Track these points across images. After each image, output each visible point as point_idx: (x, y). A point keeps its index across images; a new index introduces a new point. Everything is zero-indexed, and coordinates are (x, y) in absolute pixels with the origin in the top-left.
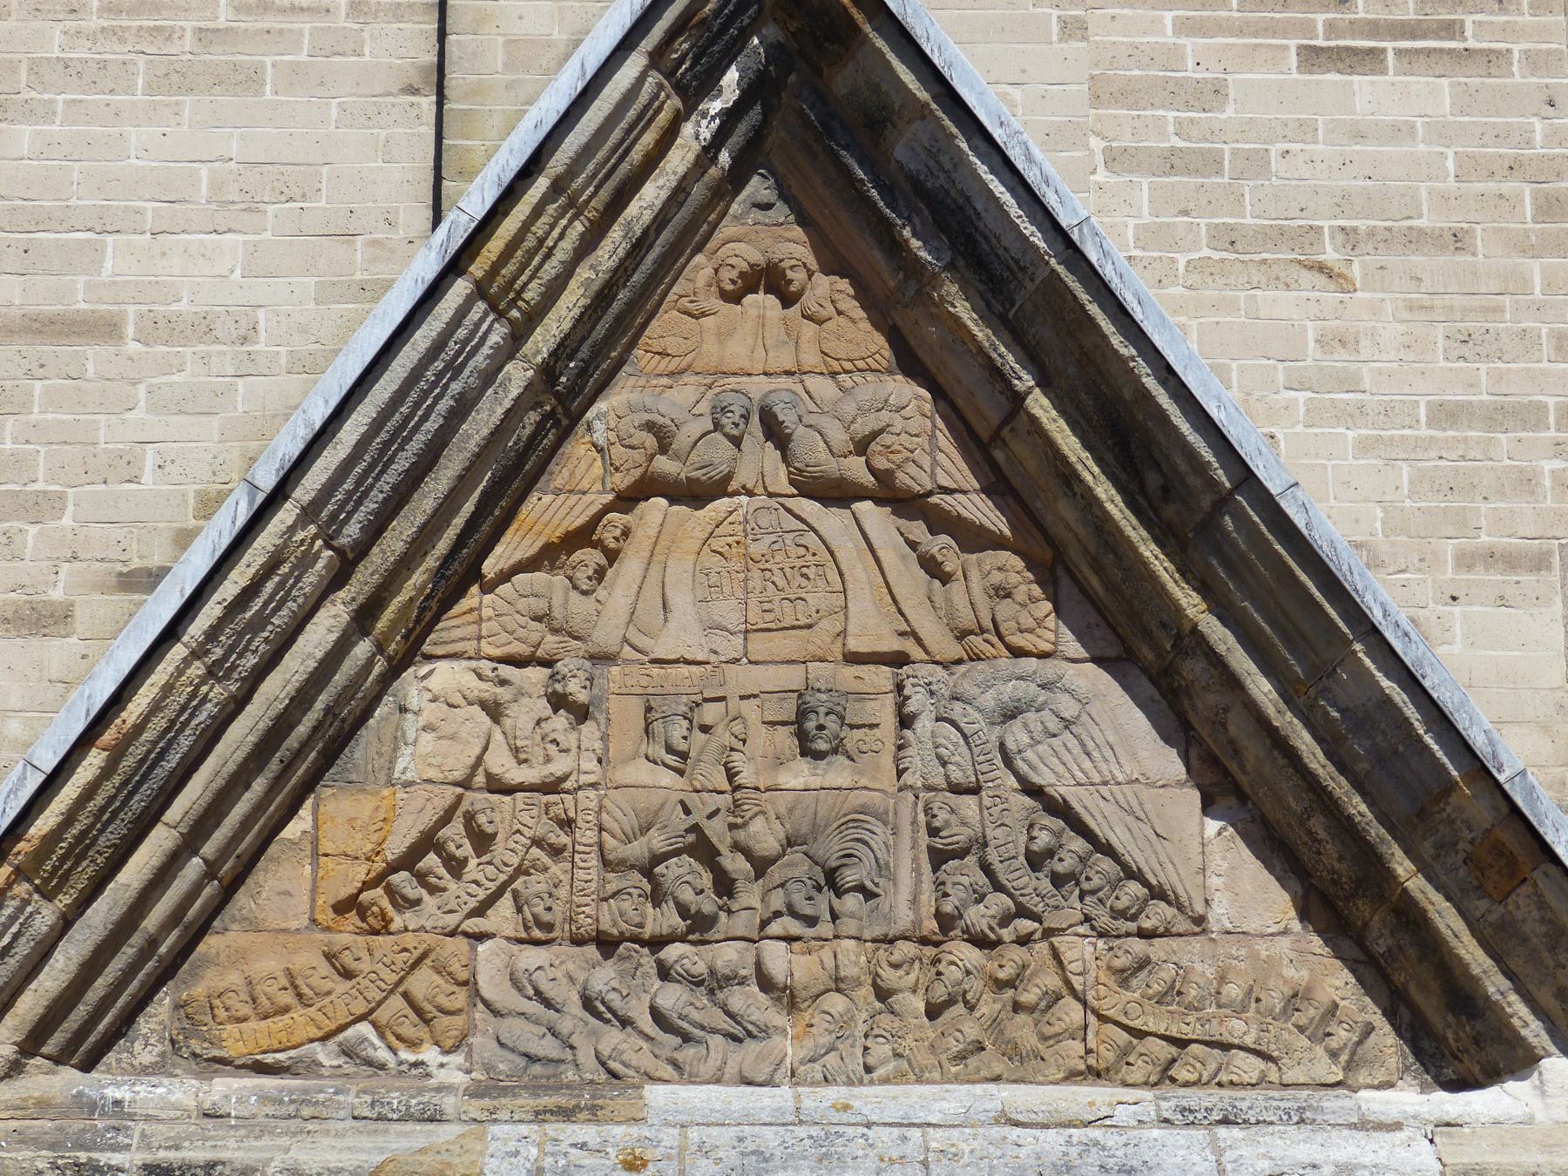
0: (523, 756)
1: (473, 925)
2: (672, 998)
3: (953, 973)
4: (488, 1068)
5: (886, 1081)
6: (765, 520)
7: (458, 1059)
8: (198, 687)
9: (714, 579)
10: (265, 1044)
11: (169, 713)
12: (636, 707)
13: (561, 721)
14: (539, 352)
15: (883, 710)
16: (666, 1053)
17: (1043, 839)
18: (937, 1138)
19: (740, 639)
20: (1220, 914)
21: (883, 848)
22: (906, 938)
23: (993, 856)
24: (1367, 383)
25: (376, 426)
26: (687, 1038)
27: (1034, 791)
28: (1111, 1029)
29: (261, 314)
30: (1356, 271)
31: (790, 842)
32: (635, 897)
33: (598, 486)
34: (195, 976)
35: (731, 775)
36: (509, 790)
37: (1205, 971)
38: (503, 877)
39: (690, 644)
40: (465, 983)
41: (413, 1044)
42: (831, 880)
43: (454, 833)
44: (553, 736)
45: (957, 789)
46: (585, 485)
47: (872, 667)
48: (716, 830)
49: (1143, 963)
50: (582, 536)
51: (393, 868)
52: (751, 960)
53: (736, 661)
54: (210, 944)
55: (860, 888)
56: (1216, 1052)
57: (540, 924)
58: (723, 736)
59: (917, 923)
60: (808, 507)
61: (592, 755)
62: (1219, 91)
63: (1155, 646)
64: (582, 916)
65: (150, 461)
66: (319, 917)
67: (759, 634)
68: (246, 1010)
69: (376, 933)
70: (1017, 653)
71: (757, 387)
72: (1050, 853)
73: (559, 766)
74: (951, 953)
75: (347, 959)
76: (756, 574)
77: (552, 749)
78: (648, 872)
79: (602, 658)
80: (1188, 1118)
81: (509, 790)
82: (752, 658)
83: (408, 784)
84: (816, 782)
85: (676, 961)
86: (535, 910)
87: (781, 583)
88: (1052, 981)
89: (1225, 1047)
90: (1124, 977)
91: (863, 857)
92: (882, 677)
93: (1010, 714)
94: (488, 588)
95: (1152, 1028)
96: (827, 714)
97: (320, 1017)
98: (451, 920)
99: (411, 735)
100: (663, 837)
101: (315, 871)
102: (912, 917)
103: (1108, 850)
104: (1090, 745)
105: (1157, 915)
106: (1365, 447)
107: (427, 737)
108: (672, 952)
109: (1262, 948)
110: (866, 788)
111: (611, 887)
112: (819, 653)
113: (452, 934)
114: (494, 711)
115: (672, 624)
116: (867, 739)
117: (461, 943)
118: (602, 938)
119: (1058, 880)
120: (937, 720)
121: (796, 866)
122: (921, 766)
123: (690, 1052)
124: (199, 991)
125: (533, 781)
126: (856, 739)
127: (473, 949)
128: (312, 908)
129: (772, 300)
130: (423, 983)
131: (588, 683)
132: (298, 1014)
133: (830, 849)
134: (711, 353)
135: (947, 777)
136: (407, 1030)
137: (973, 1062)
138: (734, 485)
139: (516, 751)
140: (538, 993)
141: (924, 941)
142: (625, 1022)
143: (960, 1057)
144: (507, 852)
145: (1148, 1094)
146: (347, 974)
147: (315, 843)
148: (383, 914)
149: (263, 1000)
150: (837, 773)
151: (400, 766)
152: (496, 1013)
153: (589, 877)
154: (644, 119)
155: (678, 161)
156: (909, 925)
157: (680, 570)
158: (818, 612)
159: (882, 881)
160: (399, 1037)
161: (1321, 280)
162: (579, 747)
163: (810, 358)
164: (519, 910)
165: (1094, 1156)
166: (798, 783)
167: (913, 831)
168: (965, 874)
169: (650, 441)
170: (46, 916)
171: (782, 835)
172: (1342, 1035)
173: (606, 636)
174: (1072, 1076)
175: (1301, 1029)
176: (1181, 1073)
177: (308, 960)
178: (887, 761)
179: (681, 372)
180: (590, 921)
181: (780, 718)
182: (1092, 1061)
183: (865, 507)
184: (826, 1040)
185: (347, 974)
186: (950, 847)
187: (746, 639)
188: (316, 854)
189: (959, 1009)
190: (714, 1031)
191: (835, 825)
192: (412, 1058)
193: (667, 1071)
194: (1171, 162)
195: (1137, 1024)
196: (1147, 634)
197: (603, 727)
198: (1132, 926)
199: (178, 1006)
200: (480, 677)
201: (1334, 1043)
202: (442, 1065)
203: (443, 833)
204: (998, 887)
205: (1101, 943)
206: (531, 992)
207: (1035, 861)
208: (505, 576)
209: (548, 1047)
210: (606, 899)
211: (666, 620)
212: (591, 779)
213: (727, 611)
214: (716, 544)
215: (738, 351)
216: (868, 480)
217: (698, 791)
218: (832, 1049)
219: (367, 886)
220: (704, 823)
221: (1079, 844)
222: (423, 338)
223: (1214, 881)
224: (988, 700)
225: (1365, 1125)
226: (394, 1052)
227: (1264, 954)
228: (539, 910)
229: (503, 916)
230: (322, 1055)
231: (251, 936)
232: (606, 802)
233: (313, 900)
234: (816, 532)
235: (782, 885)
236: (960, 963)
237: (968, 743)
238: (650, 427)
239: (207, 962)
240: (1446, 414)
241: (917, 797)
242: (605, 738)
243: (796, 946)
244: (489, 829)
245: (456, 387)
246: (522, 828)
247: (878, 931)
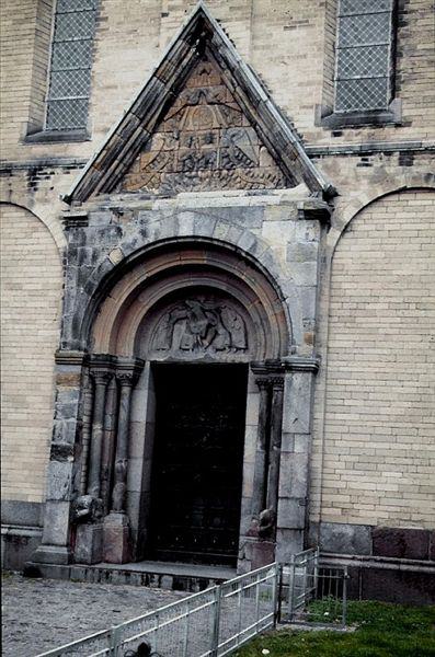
50: (178, 113)
62: (271, 35)
93: (234, 136)
114: (164, 140)
144: (166, 160)
150: (210, 146)
154: (184, 49)
155: (190, 55)
170: (100, 174)
172: (276, 181)
173: (181, 127)
177: (138, 177)
194: (263, 48)
222: (150, 86)
240: (300, 84)
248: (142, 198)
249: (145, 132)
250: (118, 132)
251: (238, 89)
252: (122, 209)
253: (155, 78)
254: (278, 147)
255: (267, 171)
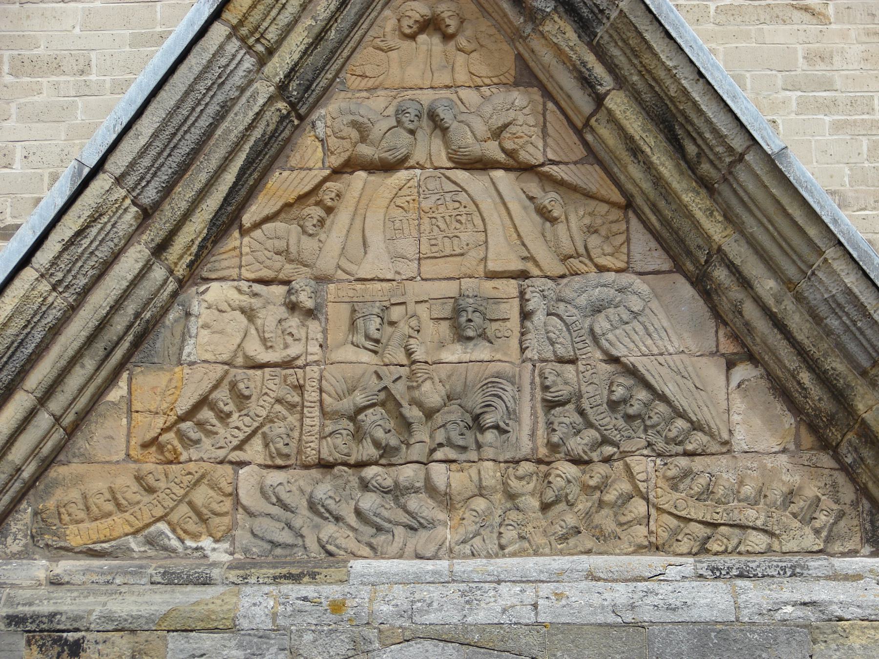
0: (269, 344)
1: (236, 456)
2: (369, 502)
3: (558, 483)
4: (246, 551)
5: (513, 555)
6: (432, 185)
7: (226, 545)
8: (45, 299)
9: (398, 225)
10: (95, 537)
11: (27, 316)
12: (345, 310)
13: (294, 322)
14: (277, 74)
15: (512, 310)
16: (366, 539)
17: (619, 392)
18: (545, 589)
19: (415, 264)
20: (741, 439)
21: (512, 401)
22: (527, 460)
23: (586, 405)
24: (838, 85)
25: (165, 123)
26: (379, 529)
27: (614, 360)
28: (666, 518)
29: (93, 55)
30: (831, 10)
31: (449, 398)
32: (344, 435)
33: (320, 165)
34: (48, 492)
35: (409, 353)
36: (261, 366)
37: (728, 478)
38: (256, 424)
39: (381, 267)
40: (230, 495)
41: (195, 536)
42: (476, 423)
43: (222, 395)
44: (289, 330)
45: (561, 361)
46: (311, 164)
47: (504, 281)
48: (399, 390)
49: (687, 473)
51: (182, 419)
52: (422, 475)
53: (412, 279)
54: (57, 472)
55: (497, 427)
56: (737, 531)
57: (280, 455)
58: (404, 328)
59: (535, 450)
60: (461, 176)
61: (315, 342)
63: (695, 261)
64: (309, 449)
65: (19, 154)
66: (132, 453)
67: (428, 261)
68: (82, 515)
69: (171, 462)
70: (601, 269)
71: (426, 97)
72: (624, 401)
73: (294, 350)
74: (557, 469)
75: (151, 480)
76: (426, 221)
77: (289, 339)
78: (353, 418)
79: (322, 279)
80: (716, 573)
81: (261, 366)
82: (424, 277)
83: (192, 364)
84: (467, 357)
85: (372, 478)
86: (278, 446)
87: (443, 226)
88: (625, 486)
89: (743, 527)
90: (674, 483)
91: (498, 407)
92: (511, 287)
93: (597, 309)
94: (244, 232)
95: (694, 517)
96: (474, 312)
97: (132, 519)
98: (221, 453)
99: (193, 331)
100: (363, 396)
101: (129, 424)
102: (531, 445)
103: (663, 398)
104: (651, 329)
105: (698, 440)
106: (837, 127)
107: (204, 332)
108: (370, 472)
109: (769, 462)
110: (500, 361)
111: (328, 430)
112: (469, 272)
113: (221, 462)
114: (249, 314)
115: (370, 255)
116: (501, 329)
117: (228, 469)
118: (322, 462)
119: (629, 418)
120: (548, 315)
121: (453, 413)
122: (536, 347)
123: (382, 538)
124: (51, 503)
125: (276, 360)
126: (493, 329)
127: (236, 473)
128: (128, 448)
129: (436, 40)
130: (202, 496)
131: (313, 295)
132: (118, 518)
133: (476, 401)
134: (395, 75)
135: (555, 352)
136: (191, 527)
137: (572, 541)
138: (411, 162)
139: (264, 340)
140: (279, 500)
141: (540, 462)
142: (338, 519)
143: (564, 538)
144: (259, 408)
145: (691, 560)
146: (150, 490)
147: (130, 403)
148: (175, 450)
149: (94, 508)
150: (482, 352)
151: (187, 350)
152: (251, 514)
153: (314, 423)
156: (529, 451)
157: (375, 219)
158: (468, 245)
159: (511, 423)
160: (185, 532)
161: (807, 17)
162: (307, 338)
163: (462, 77)
164: (267, 445)
165: (650, 600)
166: (454, 358)
167: (532, 389)
168: (567, 416)
169: (355, 134)
171: (443, 393)
172: (822, 519)
173: (326, 263)
174: (639, 549)
175: (795, 515)
176: (715, 547)
177: (125, 482)
178: (514, 343)
179: (375, 88)
180: (314, 452)
181: (443, 316)
182: (653, 539)
183: (499, 174)
184: (473, 528)
185: (150, 490)
186: (557, 399)
187: (419, 264)
188: (130, 411)
189: (562, 506)
190: (398, 524)
191: (479, 386)
192: (194, 545)
193: (366, 551)
195: (683, 514)
196: (689, 253)
197: (323, 324)
198: (680, 449)
199: (36, 513)
200: (240, 291)
201: (817, 524)
202: (214, 550)
203: (213, 396)
204: (590, 425)
205: (658, 461)
206: (274, 500)
207: (613, 405)
208: (257, 225)
209: (285, 537)
210: (325, 438)
211: (366, 253)
212: (316, 358)
213: (407, 246)
214: (399, 201)
215: (413, 75)
216: (501, 157)
217: (387, 365)
218: (477, 534)
219: (165, 430)
220: (391, 386)
221: (642, 395)
223: (735, 418)
224: (582, 300)
225: (835, 577)
226: (182, 541)
227: (769, 465)
228: (280, 445)
229: (255, 451)
230: (133, 543)
231: (85, 466)
232: (325, 373)
233: (128, 442)
234: (466, 191)
235: (444, 426)
236: (563, 475)
237: (568, 330)
238: (355, 124)
239: (56, 483)
241: (534, 366)
242: (325, 332)
243: (454, 466)
244: (246, 393)
245: (220, 98)
246: (268, 391)
247: (508, 456)
248: (171, 579)
249: (158, 273)
250: (43, 258)
251: (617, 102)
252: (77, 623)
253: (219, 31)
254: (836, 365)
255: (771, 474)
